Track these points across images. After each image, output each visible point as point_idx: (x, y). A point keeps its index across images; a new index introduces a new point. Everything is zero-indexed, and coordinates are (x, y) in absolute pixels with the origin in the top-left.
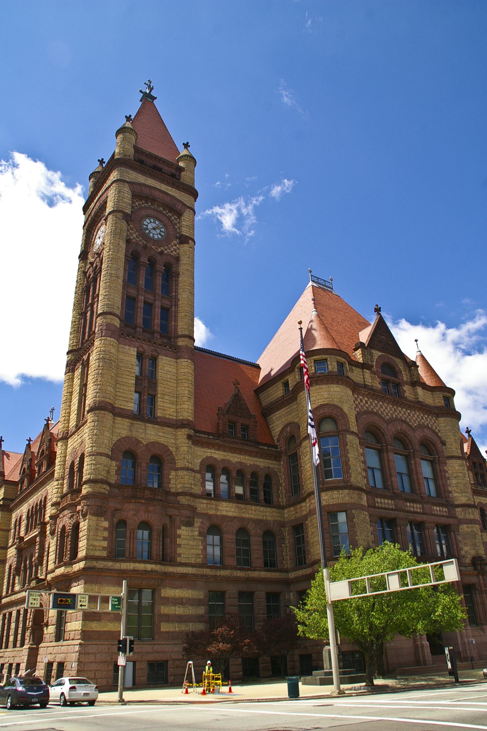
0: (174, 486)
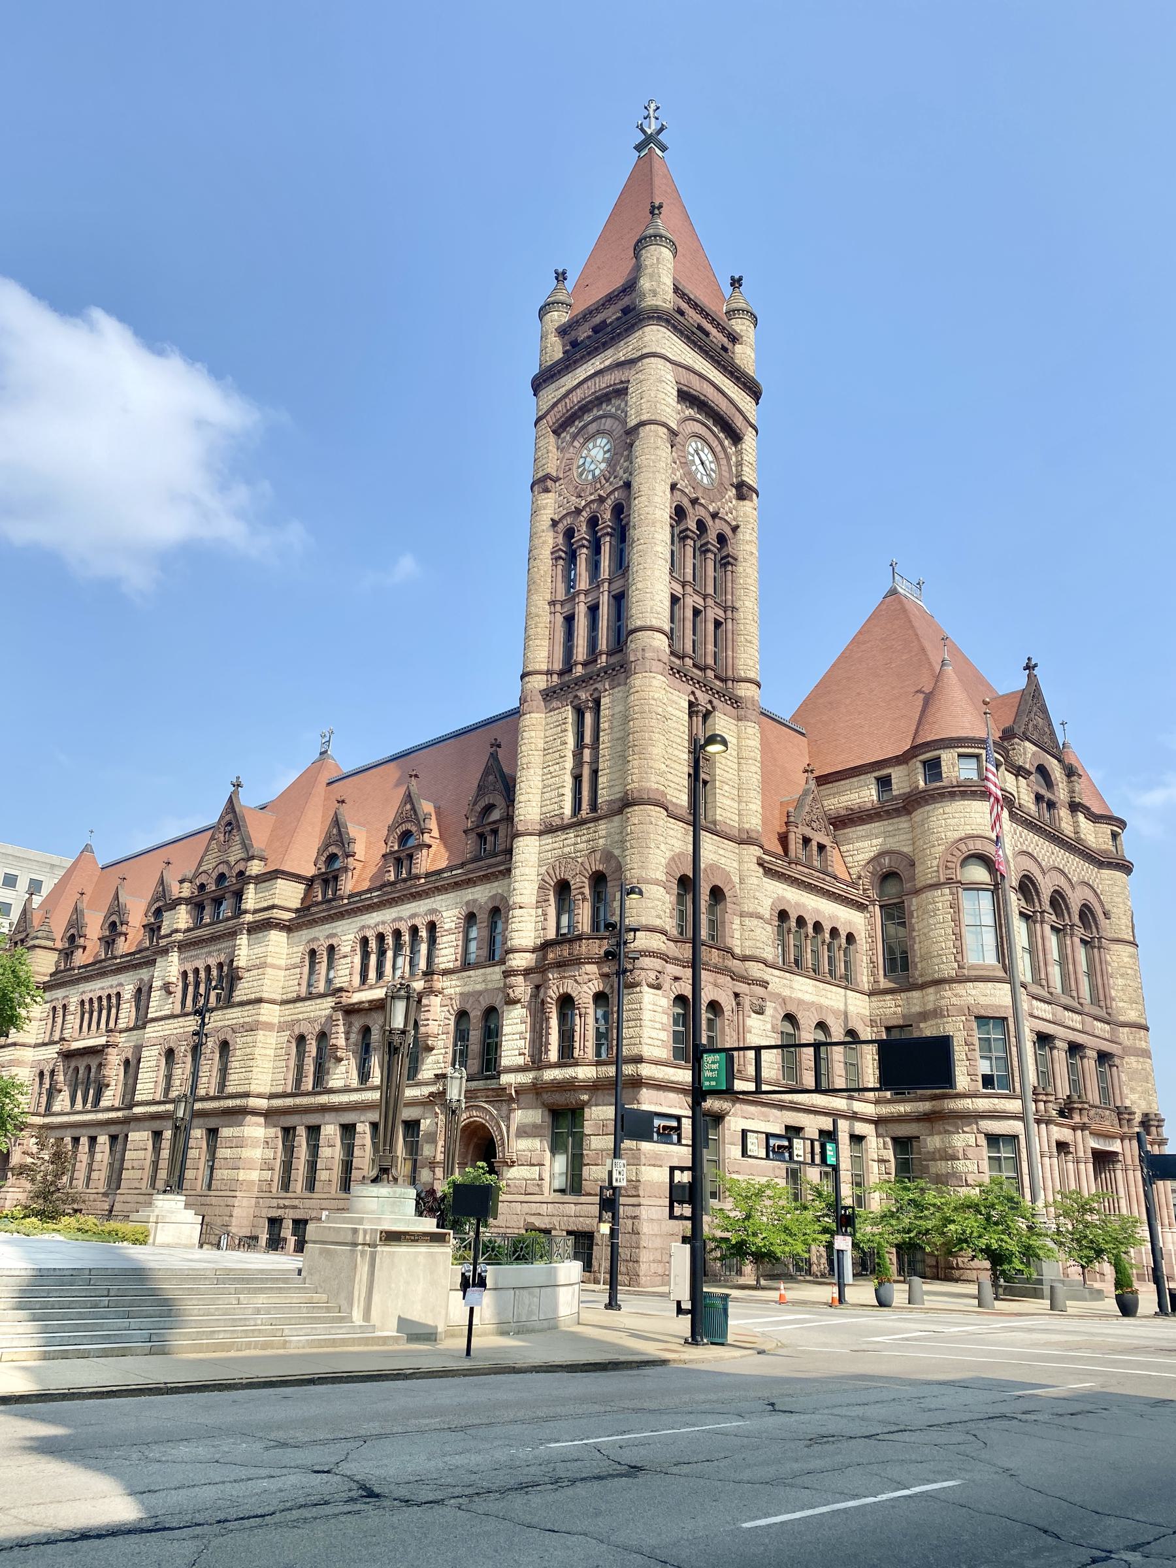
0: (738, 943)
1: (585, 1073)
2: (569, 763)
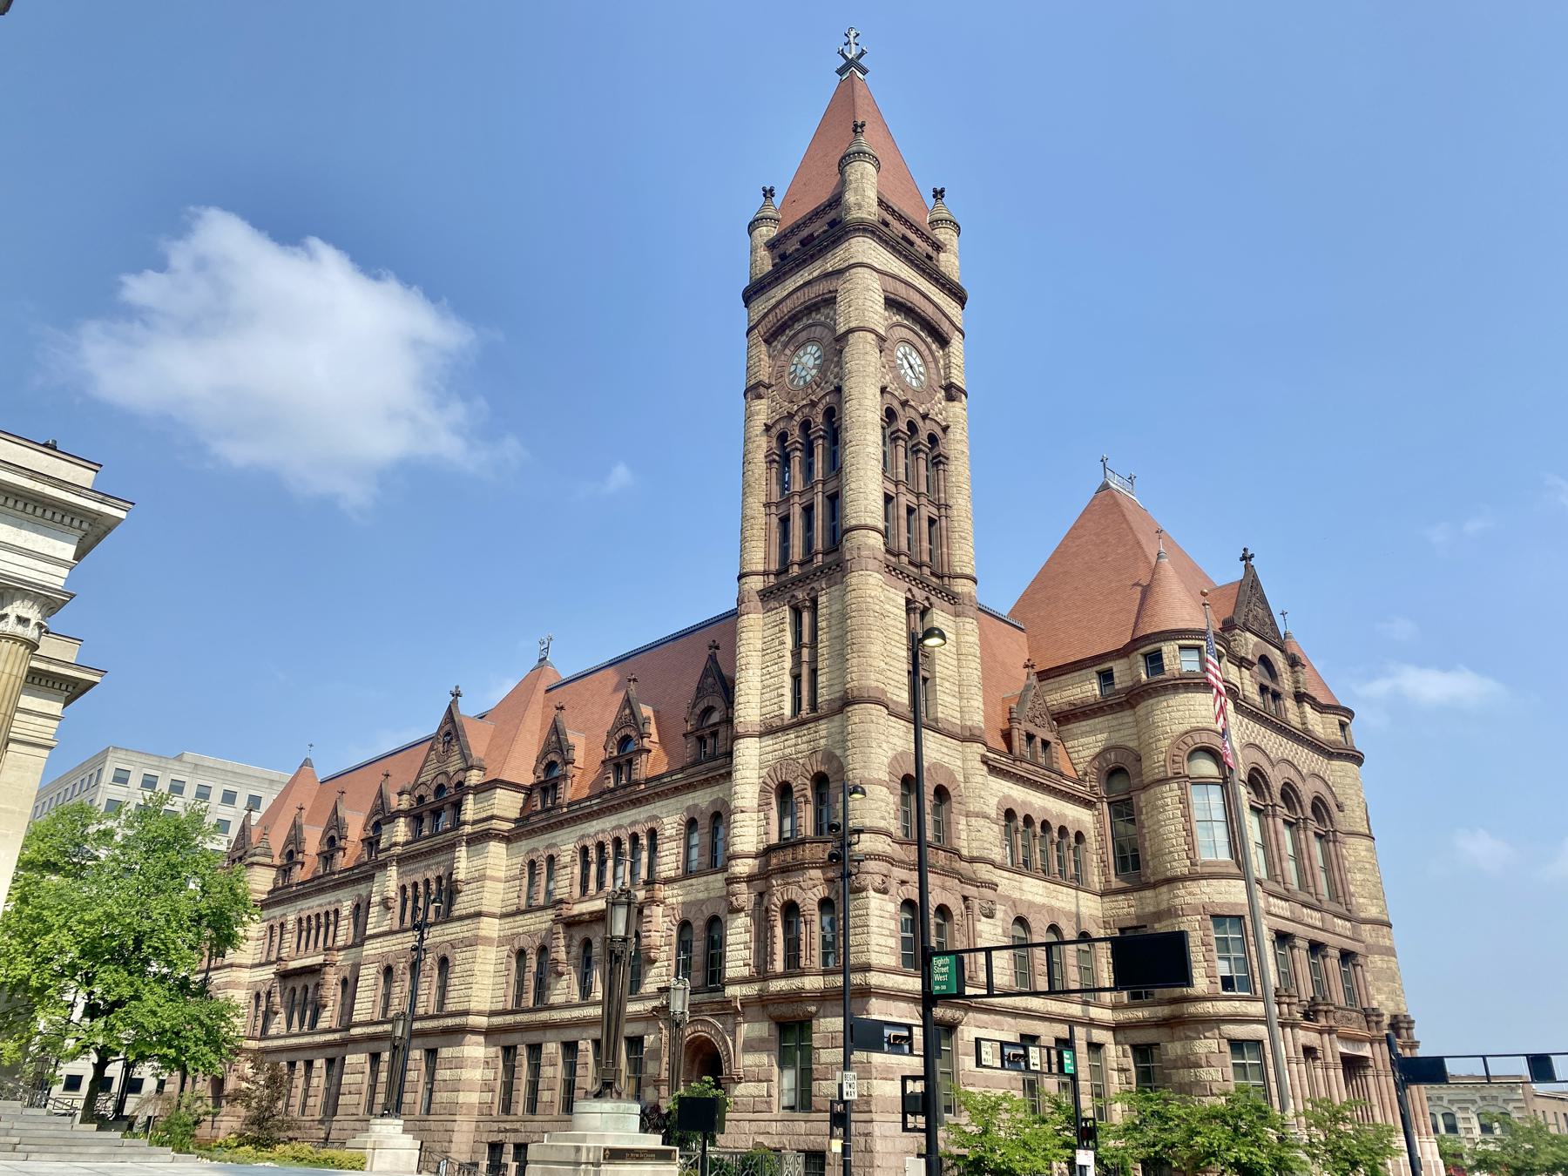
0: (965, 844)
1: (812, 983)
2: (788, 663)
